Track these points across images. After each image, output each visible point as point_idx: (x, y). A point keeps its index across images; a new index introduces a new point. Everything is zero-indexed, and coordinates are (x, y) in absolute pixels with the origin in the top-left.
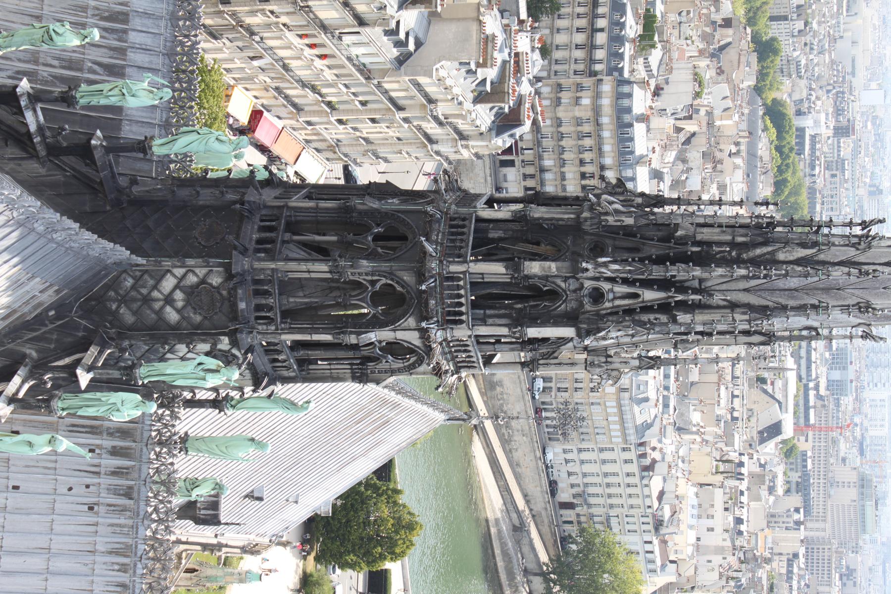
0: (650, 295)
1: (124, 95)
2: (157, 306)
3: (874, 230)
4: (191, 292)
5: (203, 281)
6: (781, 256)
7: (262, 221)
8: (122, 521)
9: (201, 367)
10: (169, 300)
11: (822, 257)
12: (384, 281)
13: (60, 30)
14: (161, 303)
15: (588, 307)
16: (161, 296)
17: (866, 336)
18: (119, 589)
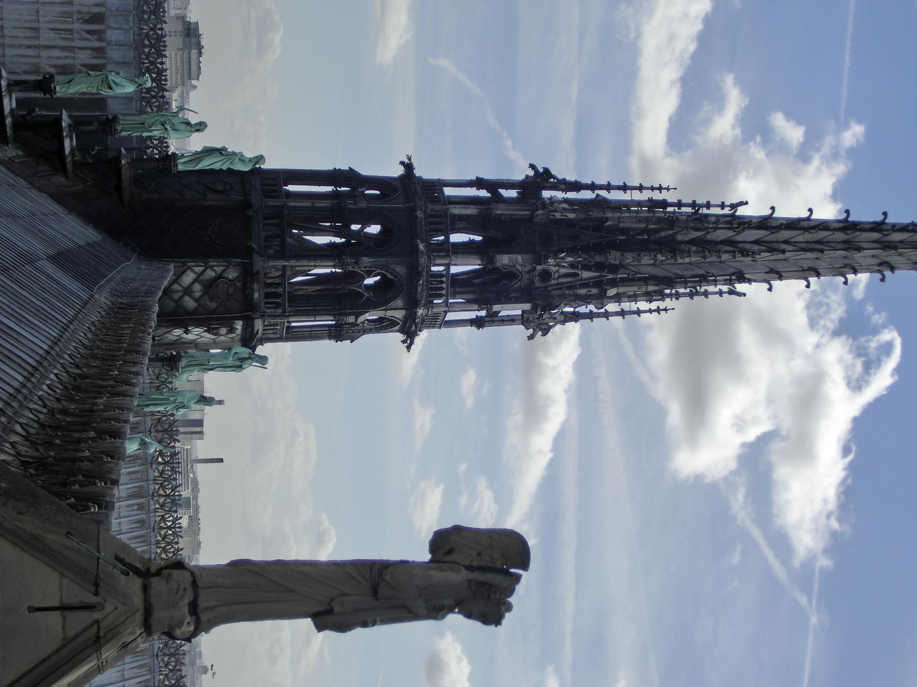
0: (586, 274)
1: (166, 129)
2: (176, 296)
3: (742, 211)
4: (209, 286)
5: (220, 276)
6: (679, 237)
7: (265, 218)
8: (136, 469)
9: (236, 356)
10: (188, 291)
11: (709, 237)
12: (379, 271)
13: (118, 80)
14: (180, 294)
15: (537, 284)
16: (180, 288)
17: (731, 292)
18: (138, 525)
